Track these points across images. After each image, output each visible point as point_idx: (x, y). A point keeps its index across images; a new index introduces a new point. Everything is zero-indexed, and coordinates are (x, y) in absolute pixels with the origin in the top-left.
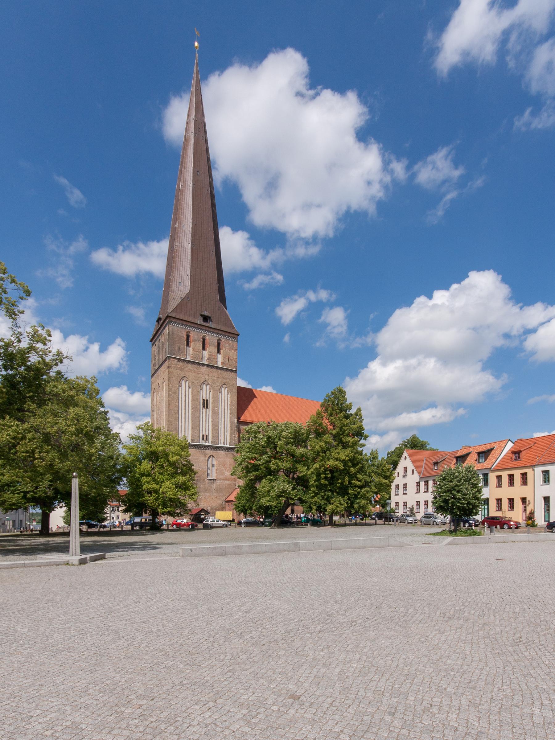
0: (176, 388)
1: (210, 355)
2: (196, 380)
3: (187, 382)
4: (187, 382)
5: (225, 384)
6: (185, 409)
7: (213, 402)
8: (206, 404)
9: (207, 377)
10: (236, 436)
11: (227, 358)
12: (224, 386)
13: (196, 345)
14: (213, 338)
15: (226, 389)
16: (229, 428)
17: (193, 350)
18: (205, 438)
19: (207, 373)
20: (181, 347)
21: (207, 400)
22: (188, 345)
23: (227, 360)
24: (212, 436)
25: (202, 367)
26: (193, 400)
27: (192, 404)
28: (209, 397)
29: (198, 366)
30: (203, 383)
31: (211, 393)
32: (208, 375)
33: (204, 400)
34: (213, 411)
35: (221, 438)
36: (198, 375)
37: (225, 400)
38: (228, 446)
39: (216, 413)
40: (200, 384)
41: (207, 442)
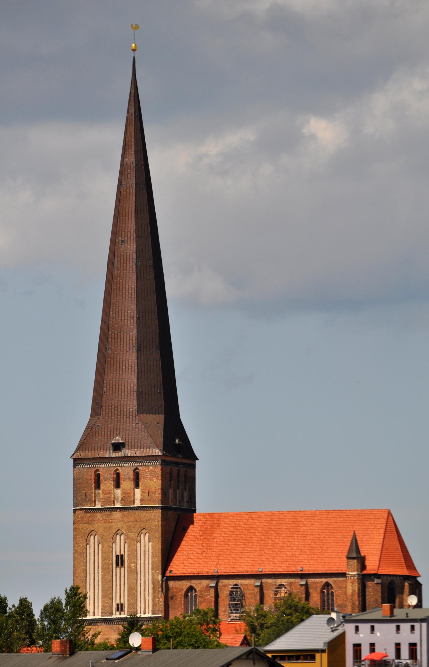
0: (82, 548)
1: (125, 493)
2: (107, 532)
4: (96, 536)
5: (144, 529)
6: (94, 573)
7: (129, 558)
9: (120, 524)
10: (161, 600)
11: (147, 491)
12: (144, 531)
14: (128, 469)
15: (147, 535)
16: (151, 591)
17: (103, 493)
18: (120, 608)
20: (88, 492)
22: (98, 487)
23: (147, 494)
24: (129, 604)
25: (114, 513)
26: (103, 559)
28: (124, 551)
29: (108, 513)
30: (116, 533)
32: (122, 521)
35: (140, 605)
36: (108, 525)
38: (150, 615)
39: (133, 572)
40: (112, 535)
41: (122, 613)
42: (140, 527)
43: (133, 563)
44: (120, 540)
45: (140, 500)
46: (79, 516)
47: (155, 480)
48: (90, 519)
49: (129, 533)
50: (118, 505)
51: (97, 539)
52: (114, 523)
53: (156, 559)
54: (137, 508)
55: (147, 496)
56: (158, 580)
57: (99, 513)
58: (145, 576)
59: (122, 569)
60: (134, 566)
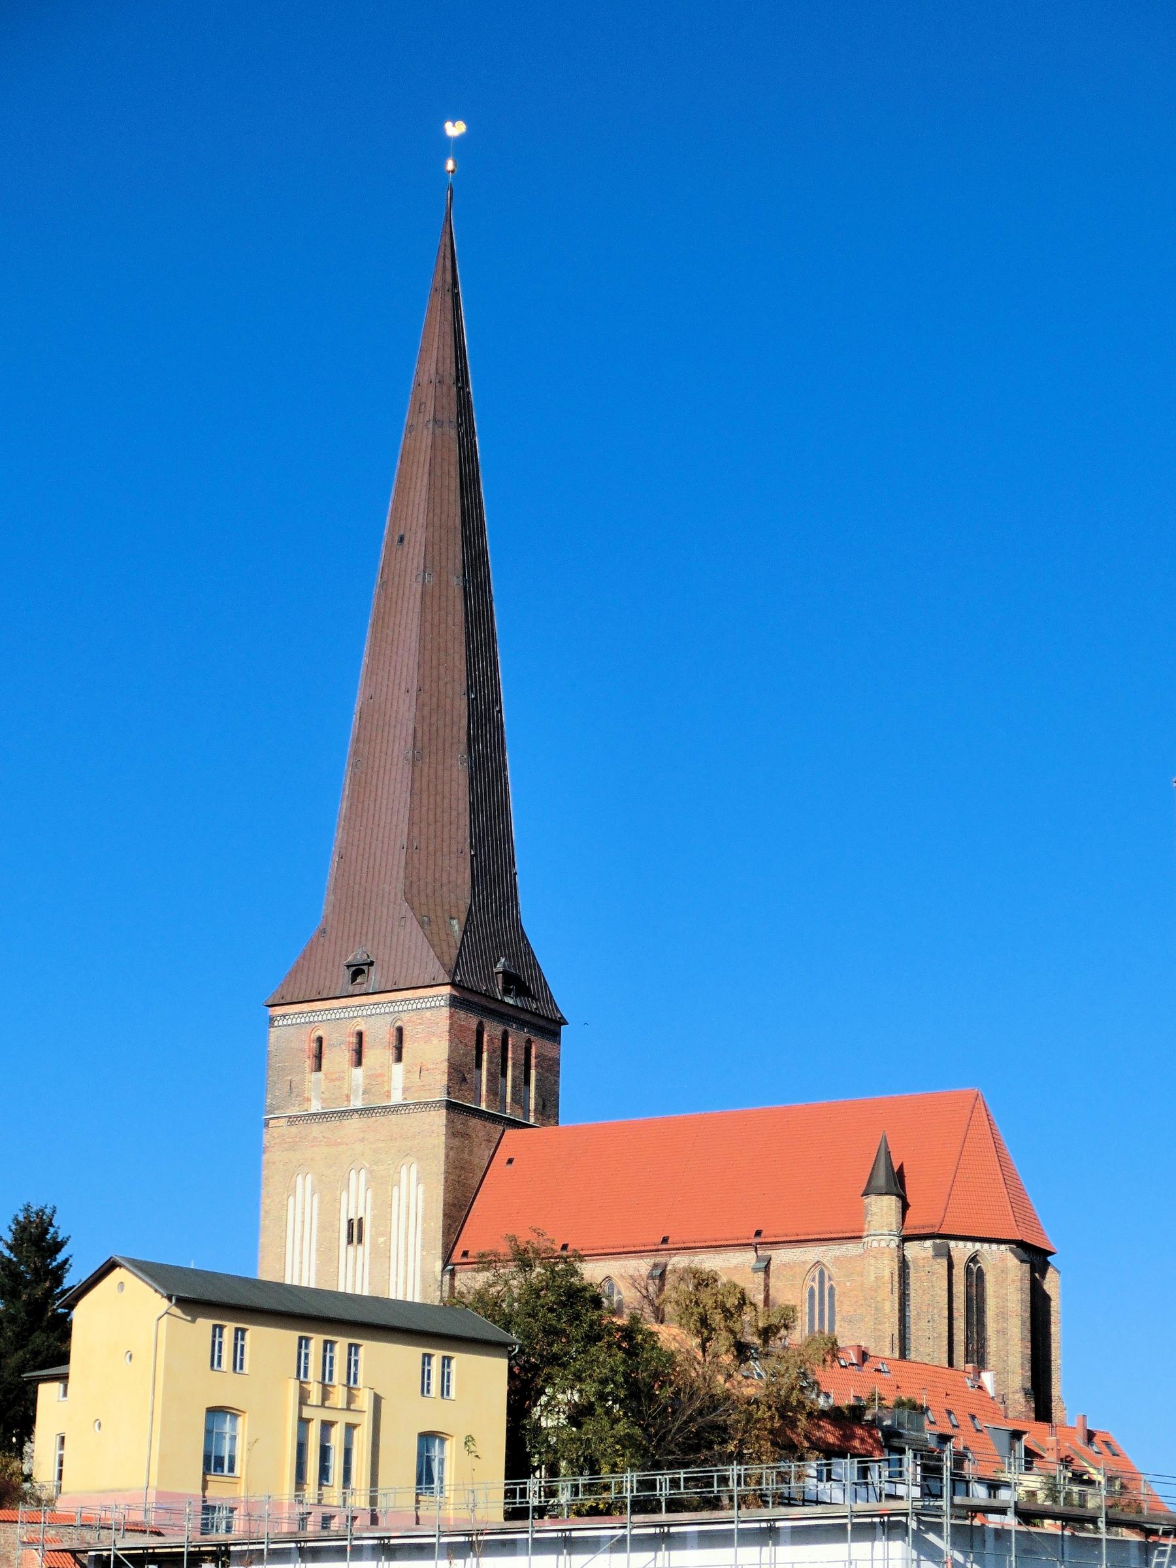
3: (309, 1177)
7: (373, 1225)
8: (355, 1232)
13: (337, 1057)
19: (361, 1136)
20: (296, 1079)
21: (360, 1220)
25: (346, 1122)
27: (318, 1241)
31: (369, 1191)
32: (362, 1140)
33: (350, 1222)
34: (374, 1246)
37: (408, 1207)
42: (399, 1151)
43: (383, 1235)
44: (358, 1182)
45: (403, 1089)
46: (275, 1135)
47: (435, 1041)
48: (297, 1139)
49: (375, 1167)
50: (357, 1103)
51: (310, 1185)
52: (347, 1144)
53: (432, 1224)
54: (395, 1109)
55: (418, 1080)
56: (434, 1272)
57: (315, 1125)
58: (406, 1264)
59: (360, 1248)
60: (384, 1243)
